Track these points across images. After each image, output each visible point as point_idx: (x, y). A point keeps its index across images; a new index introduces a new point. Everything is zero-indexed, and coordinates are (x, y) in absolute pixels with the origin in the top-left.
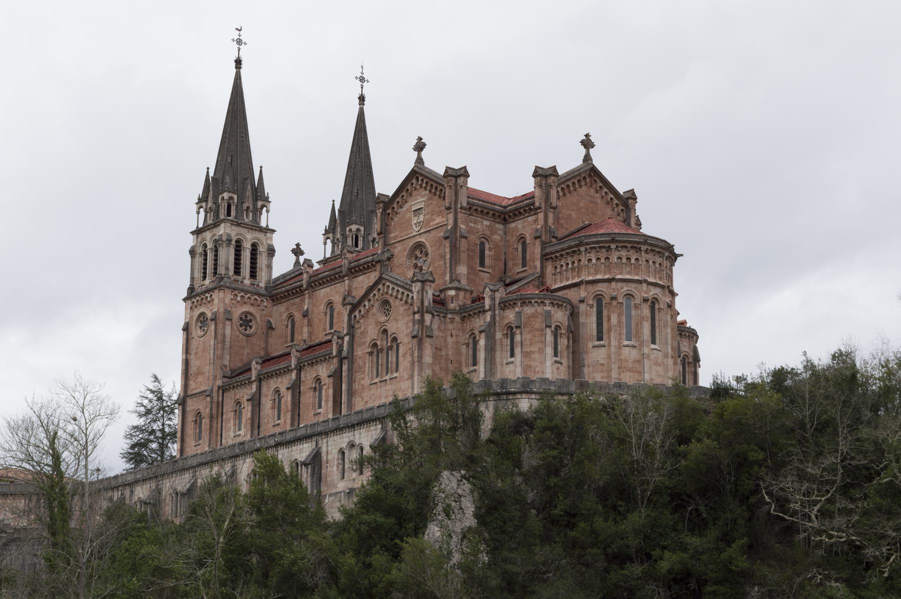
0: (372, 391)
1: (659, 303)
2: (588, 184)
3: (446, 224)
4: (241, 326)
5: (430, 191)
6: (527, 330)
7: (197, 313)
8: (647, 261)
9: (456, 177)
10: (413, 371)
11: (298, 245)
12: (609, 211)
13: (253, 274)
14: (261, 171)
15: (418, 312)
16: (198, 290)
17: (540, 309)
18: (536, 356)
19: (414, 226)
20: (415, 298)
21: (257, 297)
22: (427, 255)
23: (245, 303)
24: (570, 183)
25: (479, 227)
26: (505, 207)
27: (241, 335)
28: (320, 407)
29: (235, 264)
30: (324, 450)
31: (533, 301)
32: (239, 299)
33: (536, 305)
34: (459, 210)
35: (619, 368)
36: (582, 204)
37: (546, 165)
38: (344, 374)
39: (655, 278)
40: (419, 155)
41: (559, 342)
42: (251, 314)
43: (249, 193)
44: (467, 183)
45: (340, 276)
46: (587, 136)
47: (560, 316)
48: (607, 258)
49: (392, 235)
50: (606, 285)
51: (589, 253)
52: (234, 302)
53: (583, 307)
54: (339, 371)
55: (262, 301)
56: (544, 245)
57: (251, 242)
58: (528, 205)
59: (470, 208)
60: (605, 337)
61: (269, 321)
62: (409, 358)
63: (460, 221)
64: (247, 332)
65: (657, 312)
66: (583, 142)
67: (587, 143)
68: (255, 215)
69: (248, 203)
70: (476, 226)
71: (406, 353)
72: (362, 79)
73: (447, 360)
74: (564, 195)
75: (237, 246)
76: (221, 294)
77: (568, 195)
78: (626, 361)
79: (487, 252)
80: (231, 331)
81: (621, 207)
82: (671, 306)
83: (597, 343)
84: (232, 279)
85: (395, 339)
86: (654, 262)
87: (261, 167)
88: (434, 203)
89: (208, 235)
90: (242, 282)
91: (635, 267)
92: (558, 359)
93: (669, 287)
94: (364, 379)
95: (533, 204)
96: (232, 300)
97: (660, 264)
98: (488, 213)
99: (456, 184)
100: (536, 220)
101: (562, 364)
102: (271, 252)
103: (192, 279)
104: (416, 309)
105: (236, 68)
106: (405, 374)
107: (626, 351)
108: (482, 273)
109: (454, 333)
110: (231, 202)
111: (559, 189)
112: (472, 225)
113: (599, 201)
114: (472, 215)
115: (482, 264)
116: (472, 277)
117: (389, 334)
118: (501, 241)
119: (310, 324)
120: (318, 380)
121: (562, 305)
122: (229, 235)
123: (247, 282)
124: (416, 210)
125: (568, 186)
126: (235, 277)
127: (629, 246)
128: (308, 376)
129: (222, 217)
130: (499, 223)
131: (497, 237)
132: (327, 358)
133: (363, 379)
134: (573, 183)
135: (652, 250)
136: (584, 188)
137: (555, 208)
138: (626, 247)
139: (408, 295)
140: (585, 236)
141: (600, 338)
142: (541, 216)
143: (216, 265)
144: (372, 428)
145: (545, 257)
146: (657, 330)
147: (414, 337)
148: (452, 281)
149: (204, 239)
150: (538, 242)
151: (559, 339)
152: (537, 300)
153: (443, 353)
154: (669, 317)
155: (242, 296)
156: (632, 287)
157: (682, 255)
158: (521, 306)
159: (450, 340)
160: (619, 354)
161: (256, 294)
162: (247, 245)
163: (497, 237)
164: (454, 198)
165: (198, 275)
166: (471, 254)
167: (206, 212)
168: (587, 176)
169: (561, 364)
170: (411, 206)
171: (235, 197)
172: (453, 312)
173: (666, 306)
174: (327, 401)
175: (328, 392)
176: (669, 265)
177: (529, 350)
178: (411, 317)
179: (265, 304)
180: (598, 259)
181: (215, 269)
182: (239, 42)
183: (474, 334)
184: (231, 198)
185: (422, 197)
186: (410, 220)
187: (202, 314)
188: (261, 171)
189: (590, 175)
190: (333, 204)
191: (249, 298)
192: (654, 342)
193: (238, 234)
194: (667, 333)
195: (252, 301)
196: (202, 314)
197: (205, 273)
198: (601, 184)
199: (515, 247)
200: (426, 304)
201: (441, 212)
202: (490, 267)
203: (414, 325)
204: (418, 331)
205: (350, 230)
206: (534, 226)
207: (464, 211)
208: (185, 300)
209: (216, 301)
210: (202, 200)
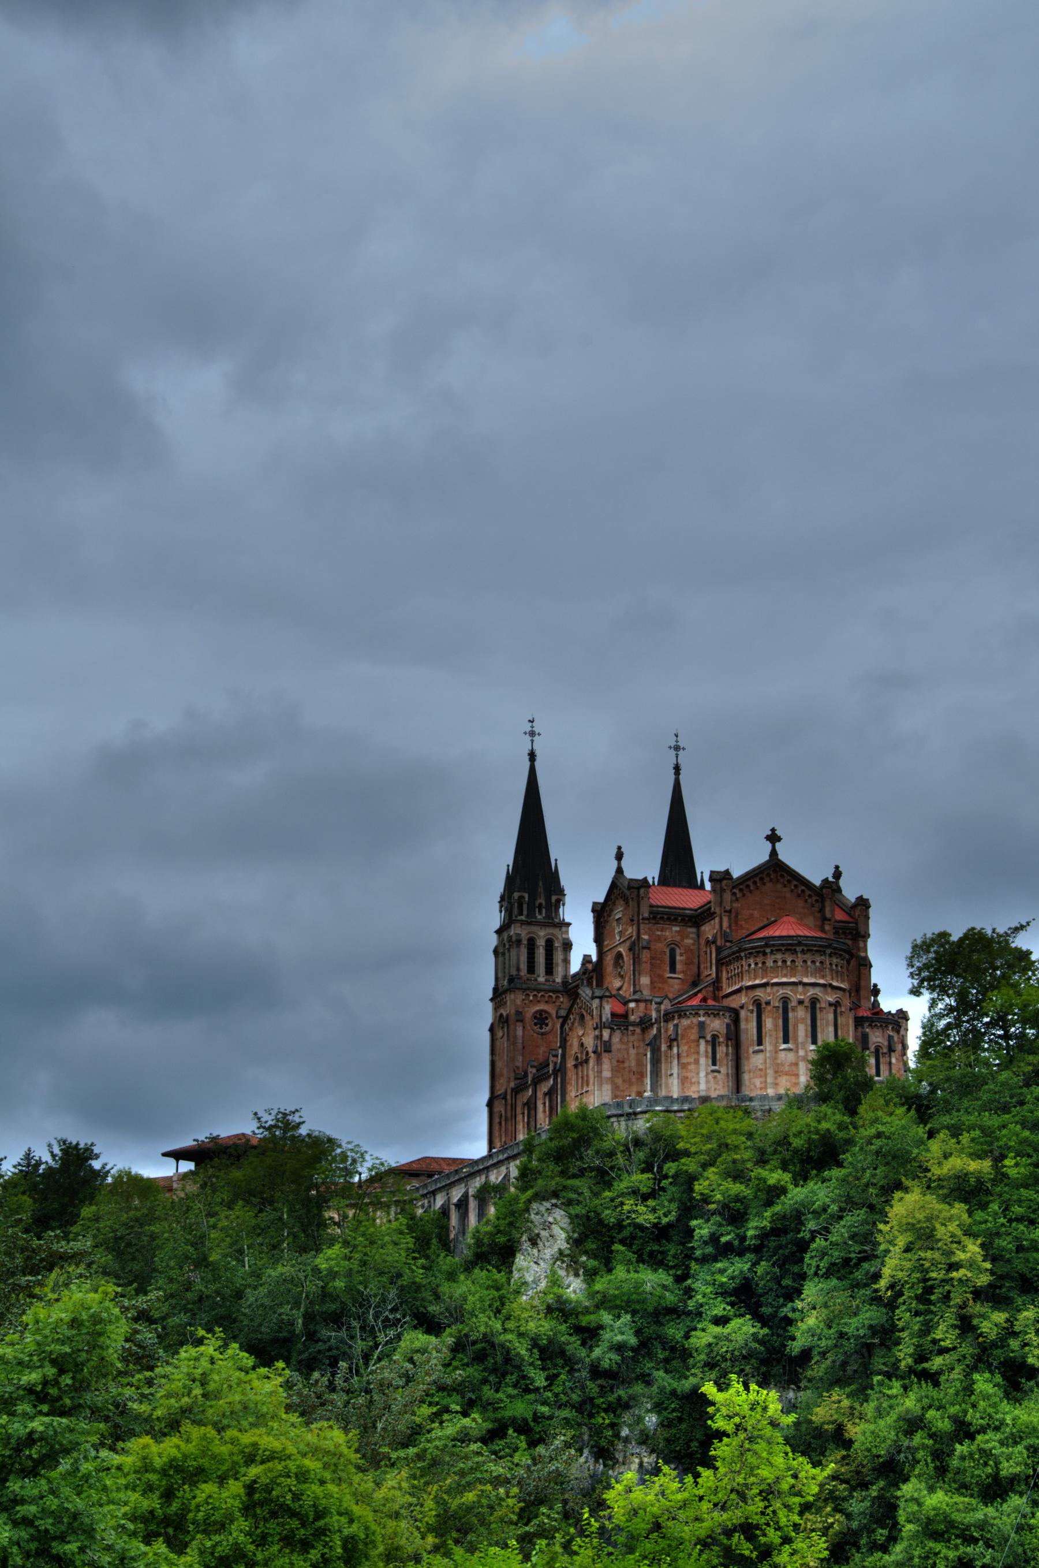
4: (536, 1024)
8: (805, 961)
9: (638, 889)
13: (550, 970)
17: (695, 1020)
18: (692, 1067)
26: (696, 910)
36: (766, 902)
37: (721, 868)
42: (546, 1012)
43: (541, 890)
46: (773, 830)
47: (717, 1025)
48: (764, 963)
49: (606, 943)
50: (762, 989)
53: (743, 1014)
56: (719, 950)
63: (642, 931)
65: (818, 1011)
66: (768, 838)
67: (773, 838)
69: (541, 900)
72: (677, 748)
73: (630, 1071)
74: (744, 895)
76: (512, 996)
78: (782, 1065)
79: (678, 958)
81: (814, 898)
83: (757, 1048)
86: (813, 962)
89: (505, 935)
90: (536, 980)
91: (792, 969)
95: (710, 908)
97: (821, 962)
99: (638, 896)
101: (719, 1072)
107: (782, 1055)
109: (636, 1044)
112: (659, 933)
113: (788, 895)
115: (673, 969)
118: (693, 944)
122: (518, 935)
131: (688, 941)
136: (769, 885)
137: (730, 911)
141: (760, 1042)
142: (717, 920)
145: (721, 963)
146: (819, 1030)
148: (635, 992)
153: (626, 1065)
155: (535, 996)
156: (788, 991)
160: (776, 1058)
161: (550, 991)
162: (541, 943)
163: (688, 941)
171: (526, 895)
172: (634, 1024)
180: (756, 964)
182: (532, 734)
184: (521, 897)
193: (529, 933)
200: (604, 1019)
202: (680, 973)
208: (492, 1000)
210: (502, 898)
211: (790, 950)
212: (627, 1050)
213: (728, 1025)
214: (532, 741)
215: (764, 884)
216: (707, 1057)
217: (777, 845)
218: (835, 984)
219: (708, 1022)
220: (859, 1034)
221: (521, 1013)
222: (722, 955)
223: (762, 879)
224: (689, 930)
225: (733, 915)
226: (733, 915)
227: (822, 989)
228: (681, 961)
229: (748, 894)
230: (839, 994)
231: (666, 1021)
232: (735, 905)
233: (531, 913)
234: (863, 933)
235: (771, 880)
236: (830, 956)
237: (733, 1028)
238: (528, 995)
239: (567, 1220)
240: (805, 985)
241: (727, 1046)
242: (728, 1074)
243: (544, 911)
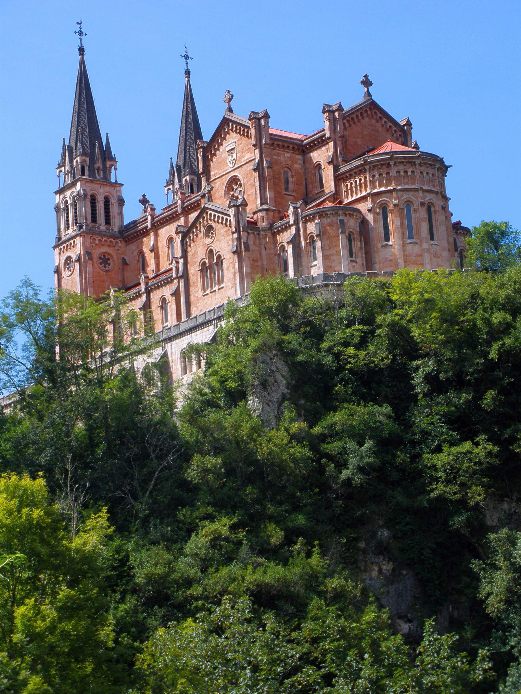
0: (205, 301)
2: (370, 116)
3: (254, 159)
5: (240, 133)
6: (325, 237)
7: (64, 257)
8: (421, 172)
10: (235, 280)
11: (144, 196)
13: (108, 221)
14: (107, 137)
15: (236, 232)
16: (64, 238)
19: (229, 164)
20: (232, 220)
21: (112, 240)
22: (240, 185)
23: (103, 245)
24: (354, 116)
25: (282, 159)
27: (102, 272)
28: (167, 321)
29: (92, 214)
30: (169, 352)
31: (328, 213)
32: (97, 242)
33: (331, 216)
34: (263, 146)
35: (405, 262)
36: (365, 133)
38: (182, 290)
40: (229, 105)
41: (353, 245)
42: (108, 254)
44: (268, 122)
45: (176, 215)
48: (388, 173)
49: (212, 173)
51: (373, 170)
52: (93, 245)
54: (178, 289)
55: (116, 242)
57: (104, 195)
58: (321, 137)
59: (273, 144)
60: (391, 237)
61: (124, 259)
62: (232, 270)
64: (107, 269)
65: (433, 214)
66: (363, 82)
67: (367, 83)
68: (105, 173)
69: (99, 164)
71: (229, 267)
72: (186, 57)
74: (350, 125)
75: (92, 199)
77: (353, 125)
79: (290, 179)
80: (93, 268)
81: (399, 133)
82: (445, 208)
84: (91, 226)
85: (219, 257)
86: (427, 173)
87: (107, 134)
88: (243, 142)
89: (68, 193)
90: (99, 228)
91: (412, 178)
92: (354, 259)
93: (441, 192)
94: (196, 292)
97: (433, 175)
98: (288, 147)
100: (328, 148)
101: (356, 262)
102: (121, 202)
103: (59, 230)
104: (234, 230)
105: (80, 55)
106: (229, 284)
107: (409, 247)
108: (286, 196)
110: (84, 164)
111: (345, 121)
112: (275, 157)
113: (380, 129)
114: (275, 149)
115: (287, 189)
116: (279, 200)
117: (214, 253)
119: (157, 257)
120: (164, 300)
121: (353, 215)
123: (103, 228)
124: (230, 150)
126: (93, 224)
127: (405, 161)
128: (156, 297)
129: (77, 177)
130: (298, 154)
131: (297, 166)
132: (169, 281)
133: (197, 292)
134: (357, 116)
135: (425, 164)
136: (367, 119)
138: (403, 162)
139: (227, 219)
140: (368, 157)
141: (387, 239)
142: (331, 144)
143: (76, 216)
144: (205, 329)
145: (339, 179)
146: (434, 229)
147: (234, 253)
149: (65, 197)
150: (331, 167)
151: (353, 243)
152: (332, 212)
154: (443, 218)
155: (100, 240)
157: (451, 166)
158: (319, 218)
161: (111, 237)
163: (297, 166)
164: (258, 136)
165: (62, 227)
166: (277, 181)
167: (65, 174)
169: (356, 262)
170: (225, 147)
171: (87, 159)
173: (440, 208)
174: (171, 315)
175: (172, 308)
176: (440, 175)
177: (328, 254)
178: (231, 237)
179: (120, 245)
180: (380, 175)
181: (76, 220)
182: (81, 33)
183: (283, 245)
184: (83, 161)
185: (234, 139)
186: (225, 159)
187: (69, 258)
188: (107, 137)
189: (370, 109)
191: (105, 241)
194: (441, 231)
195: (109, 243)
196: (69, 258)
197: (68, 224)
198: (380, 115)
199: (313, 172)
201: (249, 149)
203: (233, 242)
204: (237, 247)
205: (186, 180)
206: (327, 154)
207: (268, 146)
209: (78, 246)
211: (410, 162)
214: (81, 39)
219: (345, 221)
229: (353, 125)
231: (305, 223)
233: (92, 173)
235: (368, 116)
238: (94, 239)
239: (286, 368)
240: (424, 191)
241: (361, 241)
242: (363, 264)
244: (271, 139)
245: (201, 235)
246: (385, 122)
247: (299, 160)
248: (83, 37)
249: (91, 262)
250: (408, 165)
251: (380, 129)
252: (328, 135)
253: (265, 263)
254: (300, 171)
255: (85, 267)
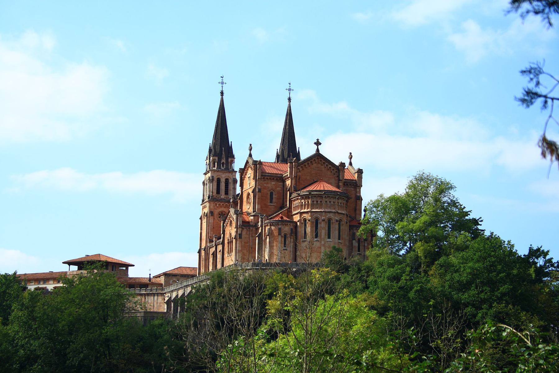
1: (332, 220)
12: (329, 173)
13: (227, 193)
14: (231, 144)
21: (227, 204)
23: (221, 207)
25: (269, 185)
32: (218, 205)
39: (331, 209)
42: (224, 212)
43: (224, 156)
46: (318, 140)
49: (244, 187)
65: (331, 224)
66: (315, 143)
67: (318, 143)
69: (224, 161)
70: (268, 185)
74: (303, 169)
77: (305, 169)
79: (274, 196)
86: (330, 202)
96: (214, 206)
98: (274, 179)
101: (287, 250)
108: (269, 206)
112: (265, 185)
113: (323, 169)
115: (271, 202)
121: (288, 224)
123: (223, 196)
125: (305, 165)
127: (317, 196)
130: (280, 182)
131: (279, 189)
134: (308, 164)
136: (315, 165)
159: (251, 238)
161: (226, 202)
168: (316, 159)
171: (217, 158)
190: (277, 151)
191: (223, 204)
192: (329, 237)
193: (218, 176)
198: (324, 162)
202: (275, 203)
207: (260, 180)
212: (249, 238)
213: (292, 229)
214: (222, 87)
215: (312, 164)
216: (281, 243)
217: (319, 146)
218: (339, 212)
219: (283, 228)
220: (351, 233)
221: (213, 212)
222: (292, 197)
223: (311, 162)
224: (279, 183)
225: (298, 178)
226: (298, 178)
227: (333, 214)
228: (275, 198)
229: (305, 169)
230: (341, 216)
232: (299, 174)
233: (219, 167)
234: (359, 185)
235: (316, 163)
236: (338, 199)
237: (294, 230)
241: (291, 238)
243: (225, 165)
244: (262, 175)
245: (228, 225)
246: (327, 165)
247: (281, 185)
248: (224, 85)
249: (212, 217)
250: (319, 198)
251: (323, 169)
252: (289, 176)
253: (251, 244)
254: (280, 191)
255: (209, 220)
